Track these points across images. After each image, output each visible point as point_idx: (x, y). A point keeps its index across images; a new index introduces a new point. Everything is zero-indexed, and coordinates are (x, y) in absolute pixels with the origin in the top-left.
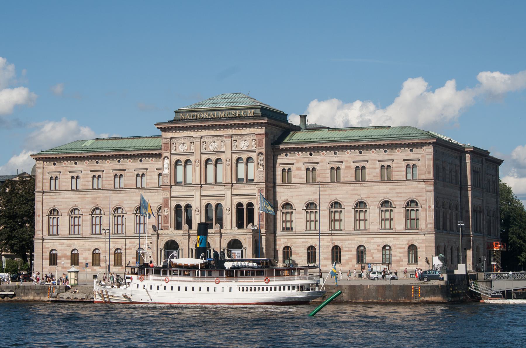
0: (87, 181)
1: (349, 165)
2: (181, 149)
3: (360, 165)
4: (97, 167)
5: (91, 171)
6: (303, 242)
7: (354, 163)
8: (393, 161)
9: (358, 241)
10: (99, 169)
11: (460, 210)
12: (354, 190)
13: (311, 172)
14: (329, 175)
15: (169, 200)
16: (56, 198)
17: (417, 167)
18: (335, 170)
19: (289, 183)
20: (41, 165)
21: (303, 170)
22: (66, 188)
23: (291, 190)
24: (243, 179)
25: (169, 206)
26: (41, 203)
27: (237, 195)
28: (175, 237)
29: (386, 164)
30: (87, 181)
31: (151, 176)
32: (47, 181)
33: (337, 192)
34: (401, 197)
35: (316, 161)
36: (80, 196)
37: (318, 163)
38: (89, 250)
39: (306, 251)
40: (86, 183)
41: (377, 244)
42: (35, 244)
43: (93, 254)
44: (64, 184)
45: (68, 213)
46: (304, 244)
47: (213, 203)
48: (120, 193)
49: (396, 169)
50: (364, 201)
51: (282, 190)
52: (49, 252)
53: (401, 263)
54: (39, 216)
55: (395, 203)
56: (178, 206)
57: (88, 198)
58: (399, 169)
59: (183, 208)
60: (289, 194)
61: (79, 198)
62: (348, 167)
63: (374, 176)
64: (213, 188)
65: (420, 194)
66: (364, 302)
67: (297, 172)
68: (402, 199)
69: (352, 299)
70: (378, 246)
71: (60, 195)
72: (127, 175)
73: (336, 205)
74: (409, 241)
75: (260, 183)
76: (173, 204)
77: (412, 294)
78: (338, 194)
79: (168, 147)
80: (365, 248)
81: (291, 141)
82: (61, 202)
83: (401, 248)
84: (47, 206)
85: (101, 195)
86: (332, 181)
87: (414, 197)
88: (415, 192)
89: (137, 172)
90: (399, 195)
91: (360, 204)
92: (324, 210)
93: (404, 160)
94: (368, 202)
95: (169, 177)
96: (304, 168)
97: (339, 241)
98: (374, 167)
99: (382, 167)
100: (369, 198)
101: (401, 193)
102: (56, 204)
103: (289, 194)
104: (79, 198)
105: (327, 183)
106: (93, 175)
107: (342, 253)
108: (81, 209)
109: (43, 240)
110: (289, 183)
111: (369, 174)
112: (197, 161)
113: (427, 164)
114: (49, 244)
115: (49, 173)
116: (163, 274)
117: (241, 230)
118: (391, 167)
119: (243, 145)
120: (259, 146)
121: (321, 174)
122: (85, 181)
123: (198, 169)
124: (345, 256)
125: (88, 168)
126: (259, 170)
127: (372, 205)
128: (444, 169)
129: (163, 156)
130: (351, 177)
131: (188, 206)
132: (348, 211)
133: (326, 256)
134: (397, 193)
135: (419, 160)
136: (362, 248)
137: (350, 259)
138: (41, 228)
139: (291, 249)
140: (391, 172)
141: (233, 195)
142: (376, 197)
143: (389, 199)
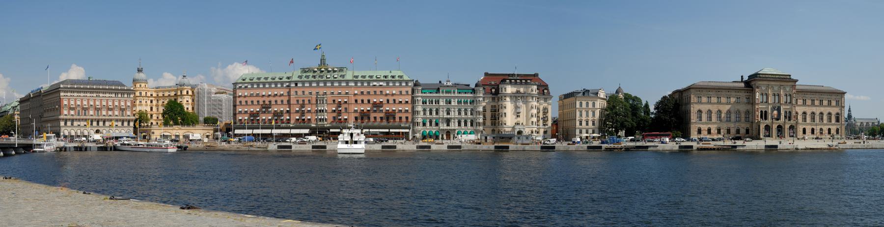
29: (830, 99)
56: (762, 112)
62: (817, 100)
91: (821, 113)
131: (766, 112)
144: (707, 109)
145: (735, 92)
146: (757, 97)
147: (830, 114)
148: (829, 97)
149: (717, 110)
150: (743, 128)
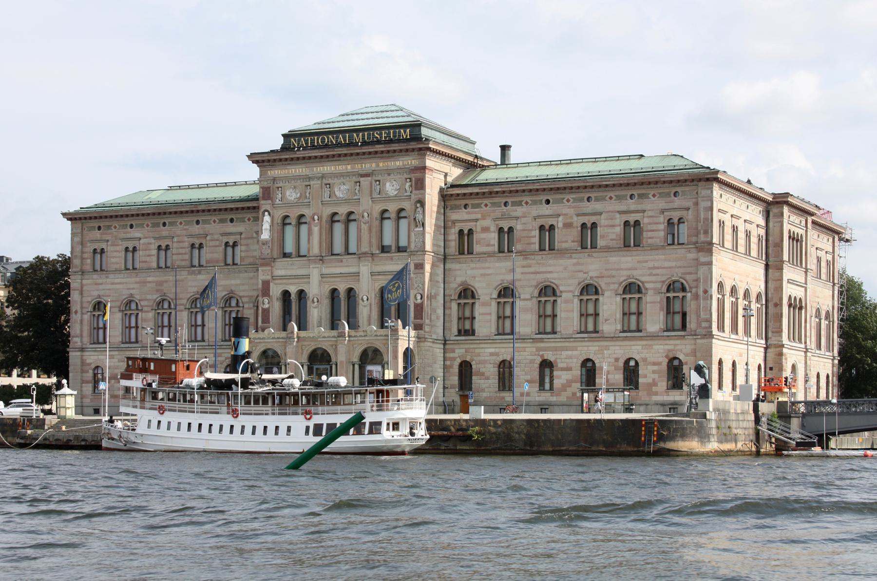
0: (149, 256)
1: (569, 221)
3: (589, 220)
4: (165, 231)
5: (155, 238)
6: (492, 354)
7: (579, 218)
8: (644, 211)
9: (582, 352)
10: (167, 235)
11: (764, 302)
12: (578, 264)
13: (506, 235)
14: (537, 240)
15: (271, 284)
16: (101, 284)
17: (686, 223)
19: (470, 252)
20: (79, 230)
21: (492, 232)
22: (118, 266)
23: (473, 265)
24: (390, 246)
25: (271, 294)
26: (78, 292)
28: (275, 345)
29: (632, 218)
30: (149, 256)
31: (247, 245)
32: (88, 255)
34: (658, 275)
35: (514, 214)
36: (138, 279)
37: (517, 218)
39: (496, 369)
40: (148, 259)
41: (615, 356)
42: (70, 358)
44: (113, 260)
45: (119, 307)
46: (494, 357)
47: (342, 288)
48: (200, 273)
49: (649, 227)
50: (594, 283)
51: (458, 266)
52: (91, 371)
53: (654, 389)
54: (76, 312)
55: (647, 286)
56: (286, 294)
57: (150, 282)
58: (654, 227)
59: (293, 296)
60: (469, 272)
61: (136, 283)
62: (568, 225)
63: (612, 240)
64: (342, 261)
65: (689, 270)
66: (553, 451)
67: (483, 236)
68: (659, 278)
69: (532, 445)
70: (617, 360)
71: (107, 277)
72: (211, 245)
73: (548, 291)
74: (669, 351)
75: (417, 252)
76: (276, 291)
77: (641, 436)
78: (550, 272)
79: (269, 194)
80: (594, 363)
81: (473, 182)
82: (109, 289)
83: (654, 364)
84: (88, 296)
87: (680, 275)
88: (680, 267)
89: (225, 239)
90: (654, 272)
92: (527, 300)
93: (663, 211)
94: (602, 284)
95: (270, 245)
96: (493, 228)
97: (551, 353)
98: (613, 224)
99: (626, 223)
100: (603, 277)
101: (658, 268)
102: (101, 293)
103: (469, 272)
104: (136, 283)
105: (533, 253)
106: (157, 245)
107: (555, 373)
108: (140, 300)
109: (82, 350)
110: (470, 252)
111: (602, 237)
112: (316, 217)
113: (702, 217)
114: (92, 358)
115: (92, 241)
116: (393, 429)
118: (641, 222)
120: (416, 189)
121: (524, 237)
122: (145, 256)
123: (316, 230)
124: (561, 378)
125: (151, 234)
126: (417, 229)
127: (608, 290)
128: (735, 229)
129: (262, 210)
130: (573, 242)
131: (301, 293)
132: (566, 301)
133: (528, 377)
134: (649, 268)
135: (688, 209)
136: (589, 364)
137: (569, 383)
138: (78, 332)
139: (471, 366)
140: (641, 232)
141: (372, 274)
142: (613, 277)
143: (636, 279)
144: (125, 294)
145: (222, 221)
146: (265, 235)
147: (548, 291)
148: (632, 205)
149: (156, 297)
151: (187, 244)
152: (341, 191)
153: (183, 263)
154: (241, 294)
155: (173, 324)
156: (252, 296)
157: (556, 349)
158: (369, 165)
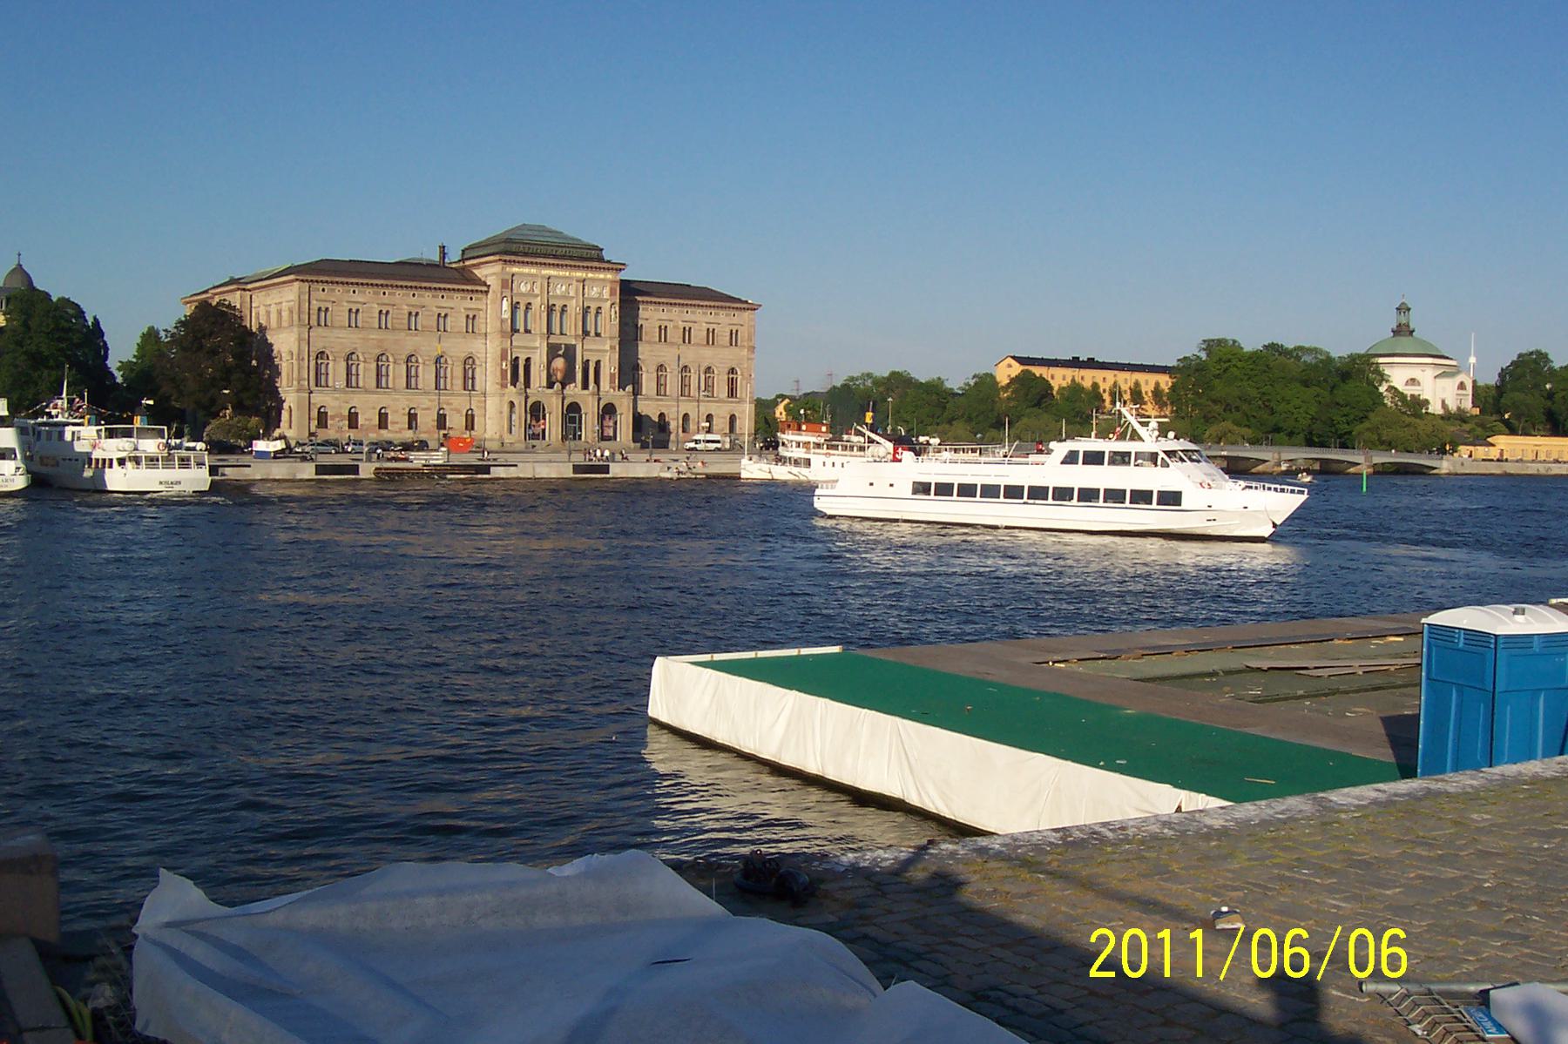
2: (523, 289)
3: (687, 326)
4: (386, 299)
18: (663, 330)
27: (587, 350)
33: (662, 354)
36: (360, 336)
38: (374, 408)
40: (370, 320)
43: (380, 413)
44: (338, 318)
48: (416, 335)
85: (389, 337)
86: (660, 340)
89: (439, 311)
105: (655, 343)
111: (695, 337)
117: (586, 392)
119: (594, 292)
148: (711, 318)
149: (379, 352)
150: (458, 411)
151: (406, 312)
152: (560, 290)
153: (402, 327)
154: (452, 354)
155: (449, 375)
156: (458, 357)
157: (667, 406)
158: (580, 274)
